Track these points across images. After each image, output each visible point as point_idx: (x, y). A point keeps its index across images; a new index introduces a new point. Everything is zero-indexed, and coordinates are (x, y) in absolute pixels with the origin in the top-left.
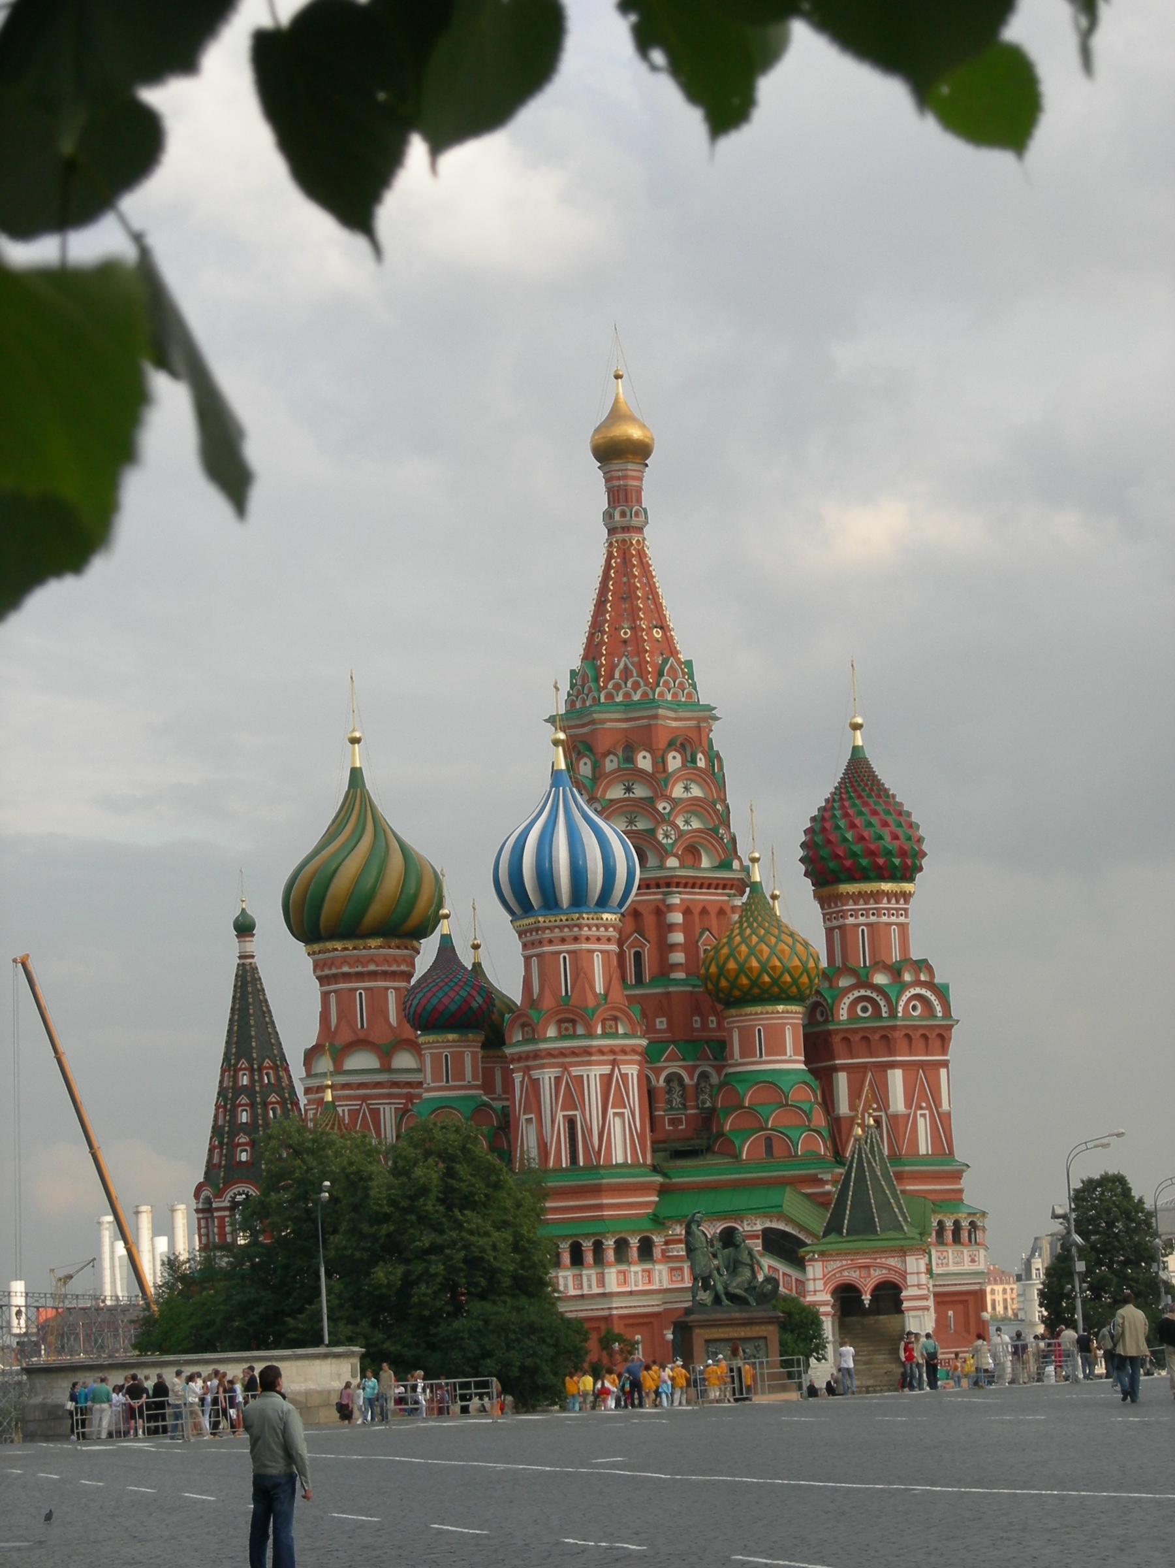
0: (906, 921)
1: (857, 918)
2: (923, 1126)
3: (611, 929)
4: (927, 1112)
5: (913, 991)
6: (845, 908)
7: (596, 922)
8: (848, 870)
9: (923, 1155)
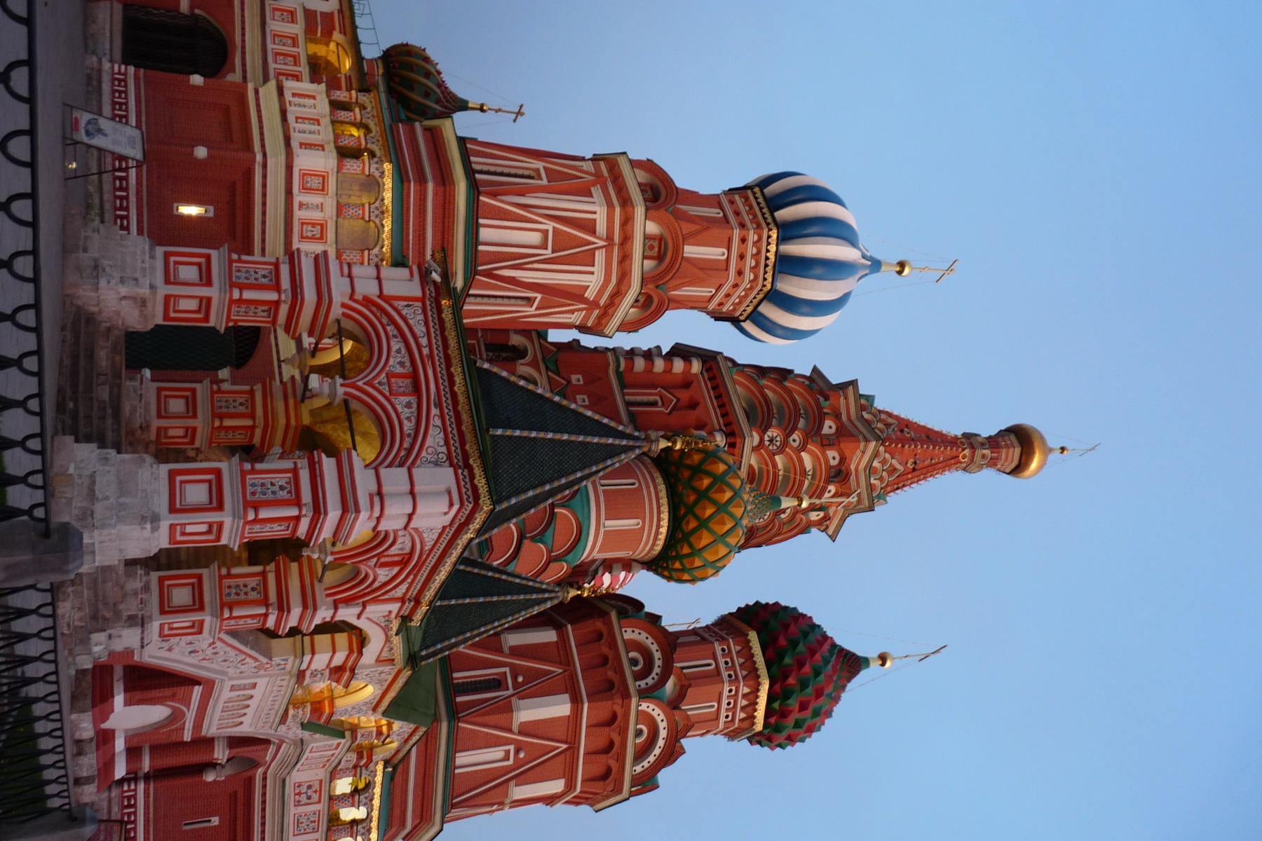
1: (723, 656)
6: (731, 640)
7: (764, 250)
8: (775, 639)
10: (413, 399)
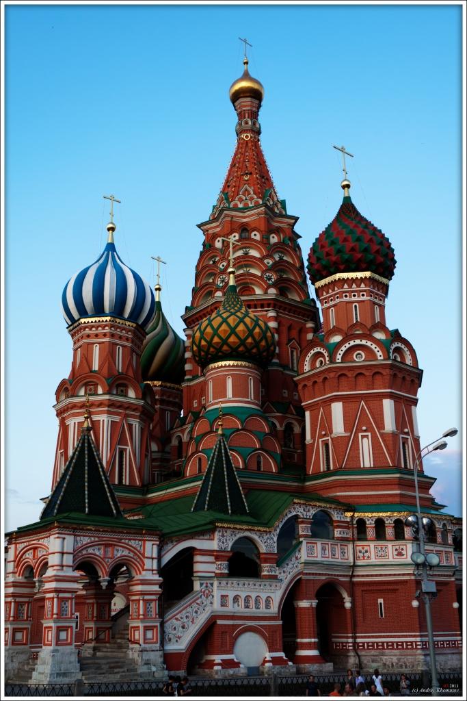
0: (369, 298)
2: (366, 446)
3: (107, 328)
4: (369, 434)
5: (352, 343)
9: (364, 468)
10: (39, 549)
